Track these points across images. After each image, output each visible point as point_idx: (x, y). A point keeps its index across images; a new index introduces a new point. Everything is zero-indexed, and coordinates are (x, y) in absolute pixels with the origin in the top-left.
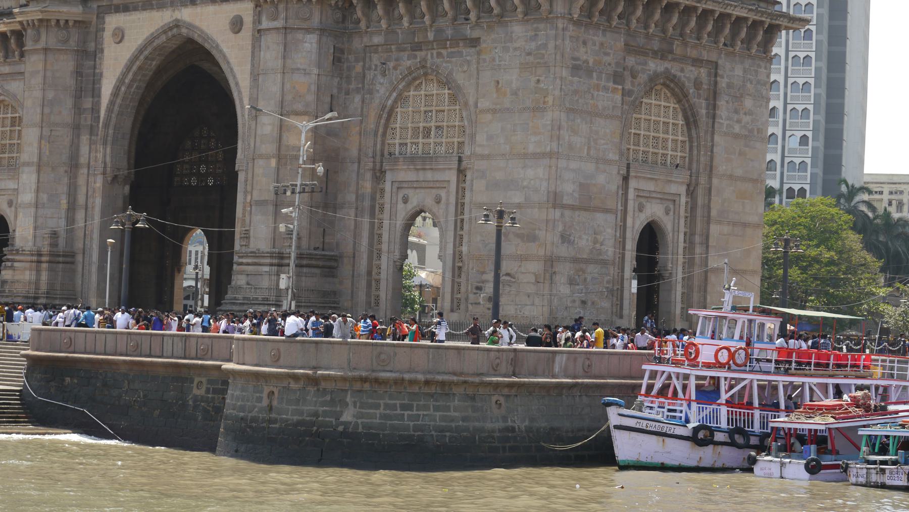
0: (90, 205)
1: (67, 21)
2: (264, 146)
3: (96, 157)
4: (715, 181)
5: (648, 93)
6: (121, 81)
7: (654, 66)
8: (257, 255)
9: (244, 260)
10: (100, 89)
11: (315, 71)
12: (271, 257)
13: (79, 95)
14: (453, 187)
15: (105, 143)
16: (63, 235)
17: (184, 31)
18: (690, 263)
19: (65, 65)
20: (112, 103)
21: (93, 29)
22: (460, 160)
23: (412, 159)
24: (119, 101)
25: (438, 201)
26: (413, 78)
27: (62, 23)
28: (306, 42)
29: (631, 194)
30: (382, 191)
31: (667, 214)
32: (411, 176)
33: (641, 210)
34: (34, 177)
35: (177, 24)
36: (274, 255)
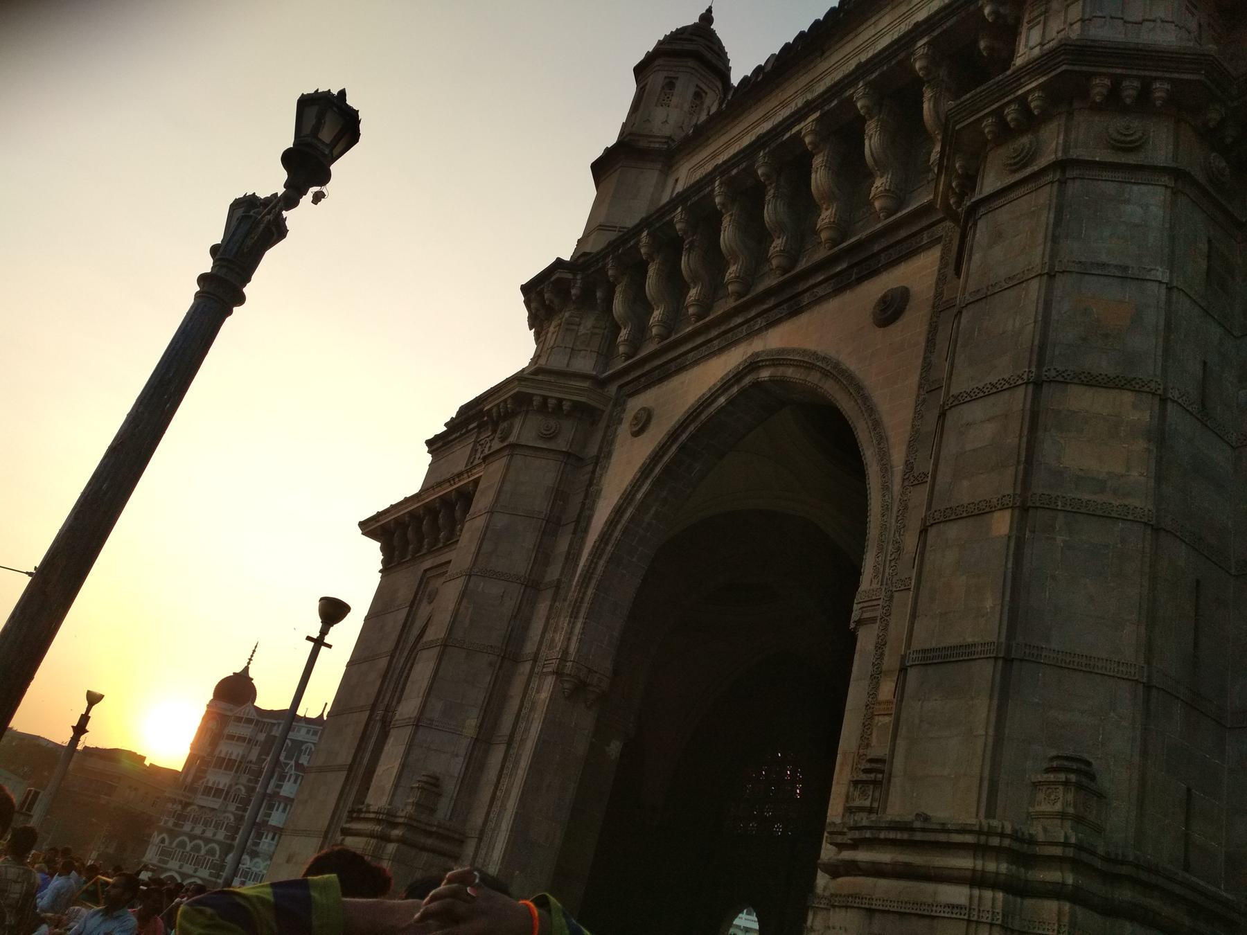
0: (517, 737)
1: (560, 401)
2: (965, 483)
3: (553, 640)
8: (918, 836)
9: (863, 856)
10: (590, 518)
12: (979, 850)
15: (574, 616)
16: (450, 787)
20: (604, 538)
21: (602, 424)
24: (617, 534)
27: (551, 403)
28: (1127, 202)
36: (995, 841)
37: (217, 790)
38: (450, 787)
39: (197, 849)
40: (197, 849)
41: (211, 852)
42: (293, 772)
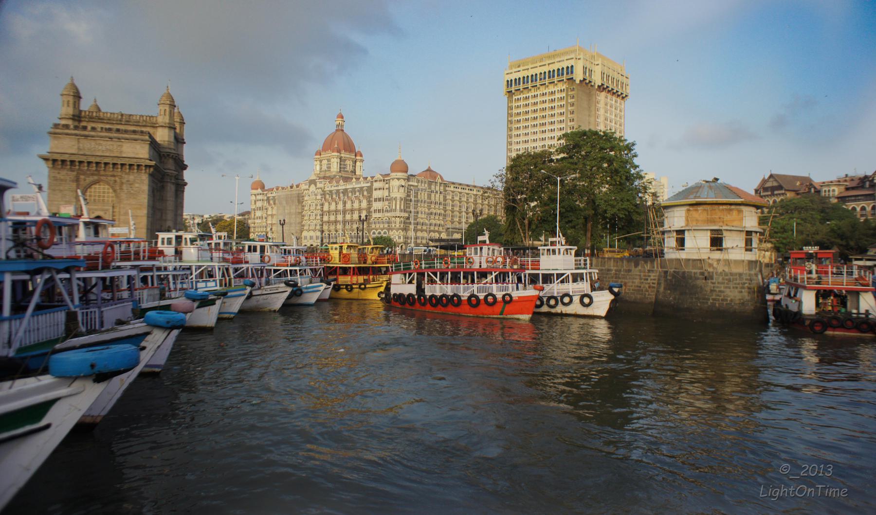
31: (106, 213)
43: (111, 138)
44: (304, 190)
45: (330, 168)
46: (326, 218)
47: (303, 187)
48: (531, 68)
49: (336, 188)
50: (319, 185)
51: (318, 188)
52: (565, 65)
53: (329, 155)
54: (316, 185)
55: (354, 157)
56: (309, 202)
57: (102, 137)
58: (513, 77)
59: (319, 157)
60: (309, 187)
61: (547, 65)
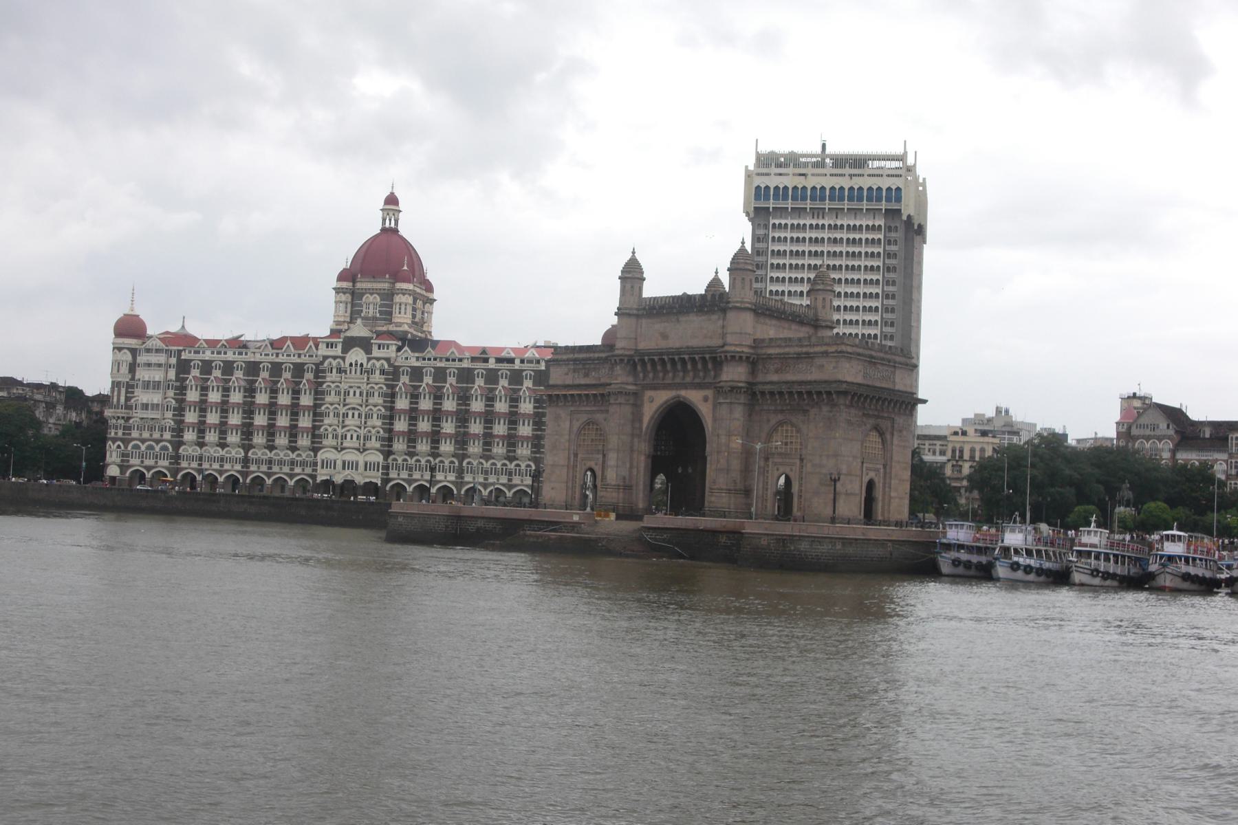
4: (893, 464)
5: (870, 431)
6: (652, 418)
7: (872, 421)
11: (742, 419)
13: (633, 421)
14: (798, 465)
16: (627, 478)
17: (682, 399)
18: (884, 494)
19: (627, 410)
22: (801, 455)
23: (780, 454)
25: (792, 470)
26: (781, 423)
29: (864, 469)
30: (768, 465)
32: (781, 460)
33: (867, 474)
34: (615, 455)
35: (678, 396)
37: (153, 405)
38: (627, 478)
39: (150, 448)
40: (150, 448)
41: (164, 448)
42: (215, 384)
43: (889, 361)
44: (325, 358)
45: (390, 313)
46: (401, 425)
47: (323, 350)
48: (813, 175)
49: (439, 364)
50: (376, 352)
51: (378, 359)
52: (885, 183)
53: (386, 286)
54: (368, 351)
55: (424, 293)
56: (344, 386)
57: (883, 359)
58: (773, 182)
59: (350, 284)
60: (346, 349)
61: (847, 176)
